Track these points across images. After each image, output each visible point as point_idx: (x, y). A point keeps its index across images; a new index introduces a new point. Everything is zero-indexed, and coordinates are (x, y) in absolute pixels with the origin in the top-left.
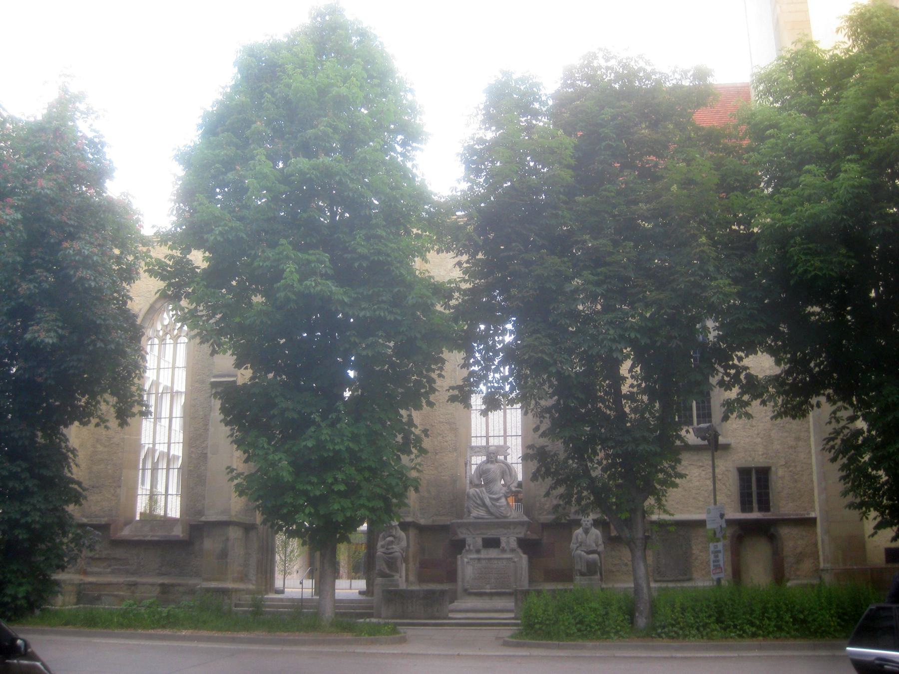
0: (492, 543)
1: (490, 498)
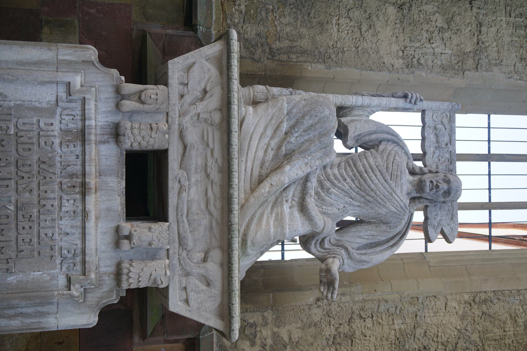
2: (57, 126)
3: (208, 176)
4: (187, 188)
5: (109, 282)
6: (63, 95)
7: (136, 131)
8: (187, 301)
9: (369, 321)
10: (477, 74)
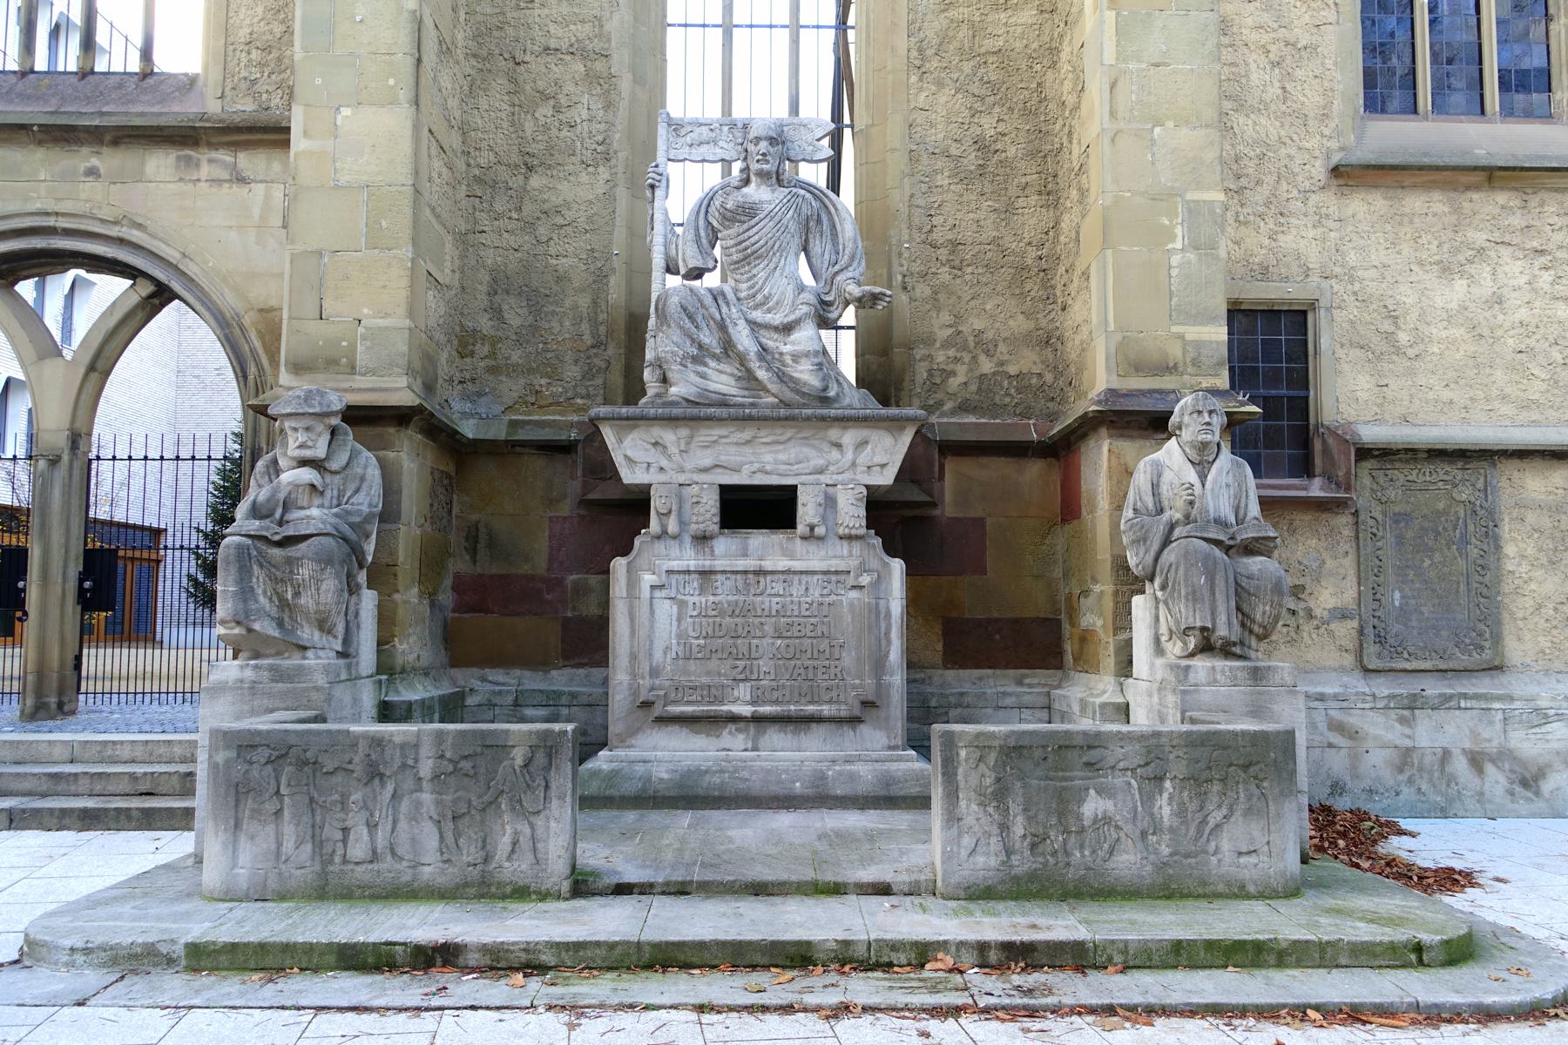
0: (759, 508)
1: (754, 325)
2: (696, 599)
3: (748, 442)
4: (762, 461)
5: (857, 547)
6: (664, 593)
7: (701, 519)
8: (883, 466)
9: (936, 221)
10: (615, 56)
